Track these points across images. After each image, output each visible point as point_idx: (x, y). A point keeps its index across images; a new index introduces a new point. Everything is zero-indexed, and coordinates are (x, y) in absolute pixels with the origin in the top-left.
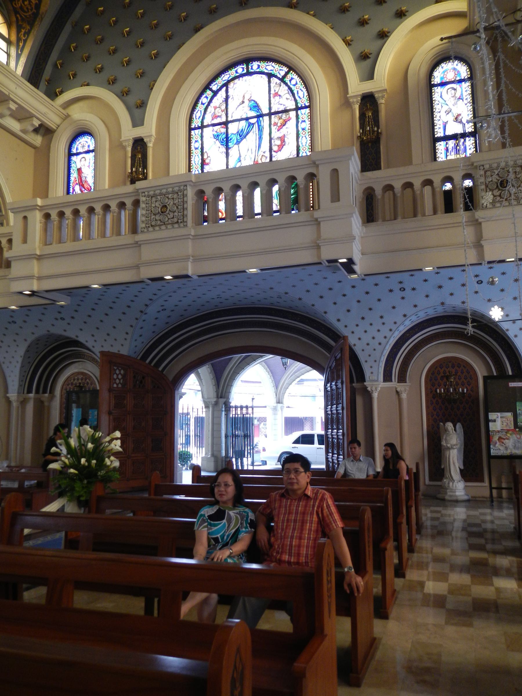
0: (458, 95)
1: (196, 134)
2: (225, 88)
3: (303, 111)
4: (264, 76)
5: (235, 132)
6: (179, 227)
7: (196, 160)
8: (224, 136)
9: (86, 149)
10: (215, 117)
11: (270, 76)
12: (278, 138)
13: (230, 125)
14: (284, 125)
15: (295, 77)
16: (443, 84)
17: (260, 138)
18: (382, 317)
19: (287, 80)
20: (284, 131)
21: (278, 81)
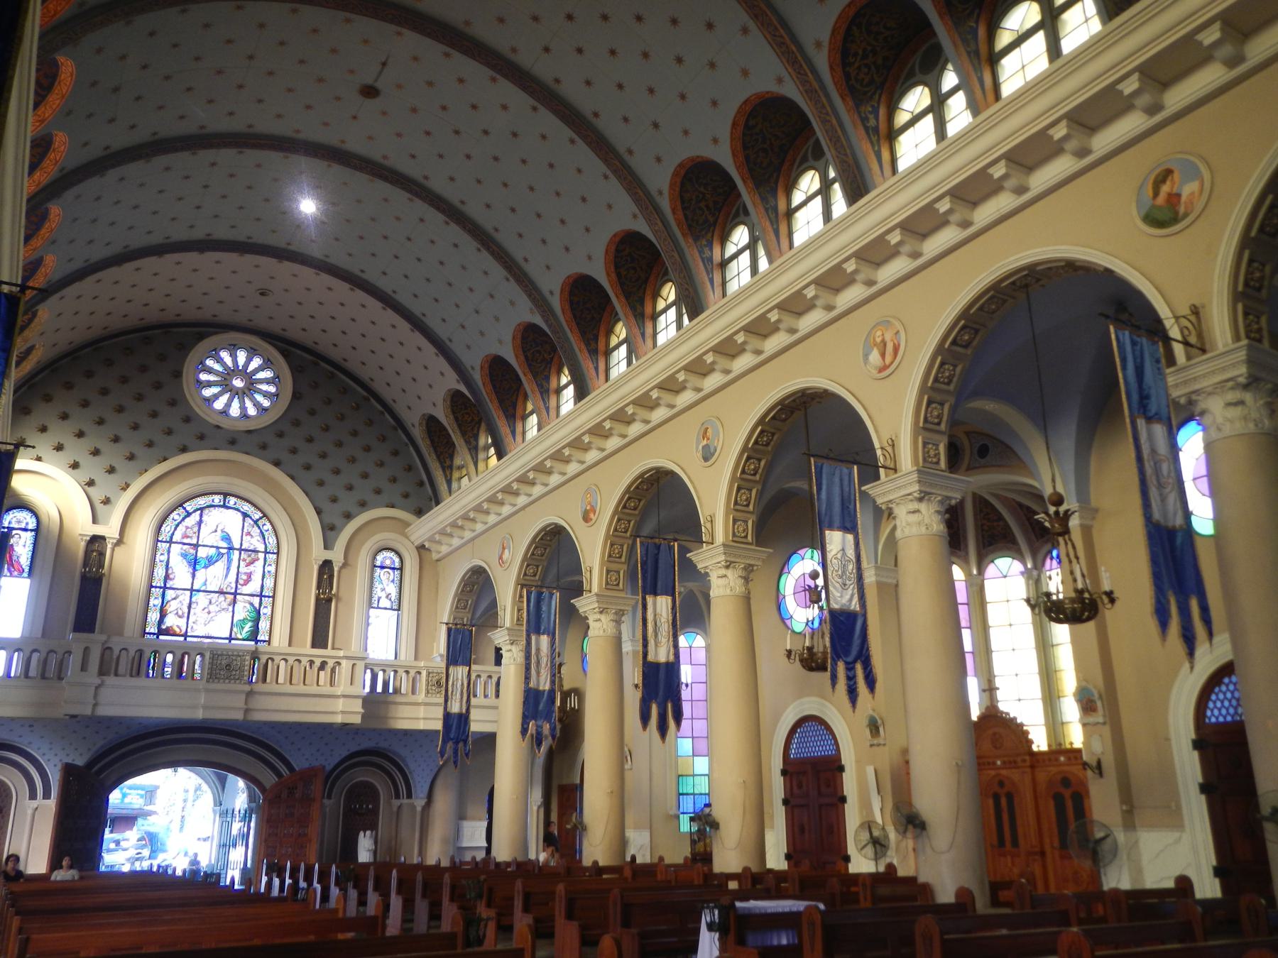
0: (391, 578)
1: (163, 547)
2: (199, 512)
3: (271, 556)
4: (239, 514)
5: (204, 556)
6: (240, 683)
7: (160, 572)
8: (192, 557)
9: (23, 526)
10: (185, 536)
11: (245, 515)
12: (245, 573)
13: (200, 548)
14: (252, 563)
15: (268, 524)
16: (382, 567)
17: (228, 569)
18: (332, 750)
19: (260, 523)
20: (251, 568)
21: (252, 523)
